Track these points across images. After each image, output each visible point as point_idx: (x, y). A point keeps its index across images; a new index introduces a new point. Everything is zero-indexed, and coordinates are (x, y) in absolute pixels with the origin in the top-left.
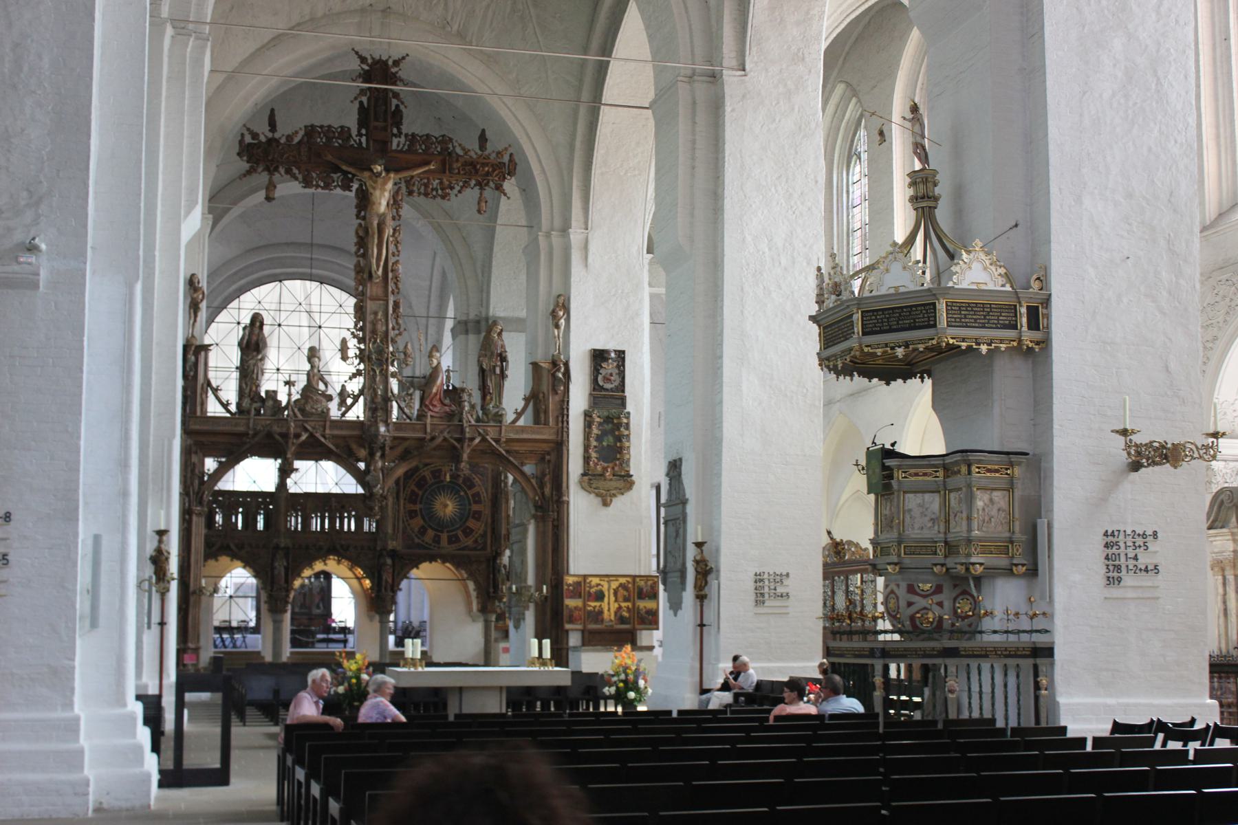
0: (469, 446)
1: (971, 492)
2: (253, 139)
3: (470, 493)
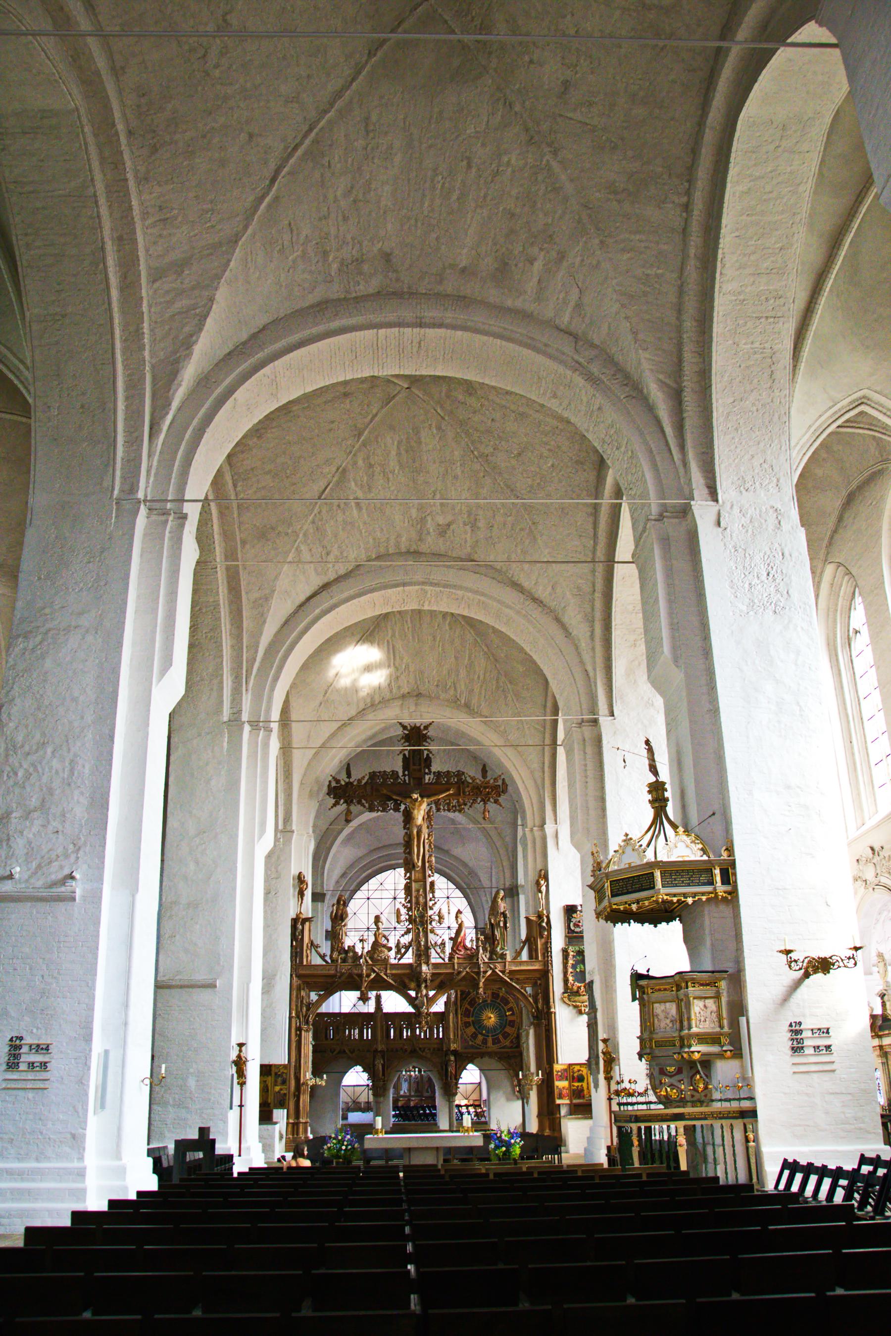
1: (689, 1001)
3: (506, 1008)
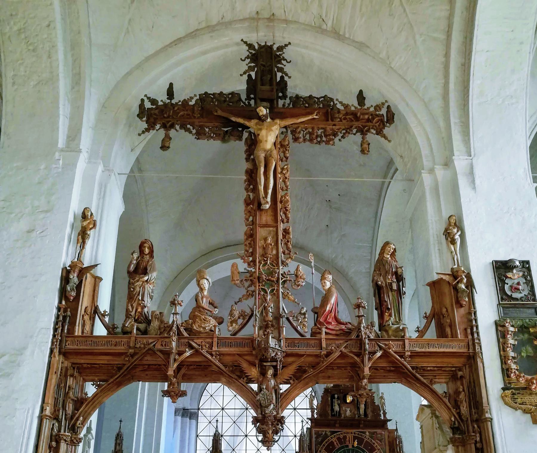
0: (370, 359)
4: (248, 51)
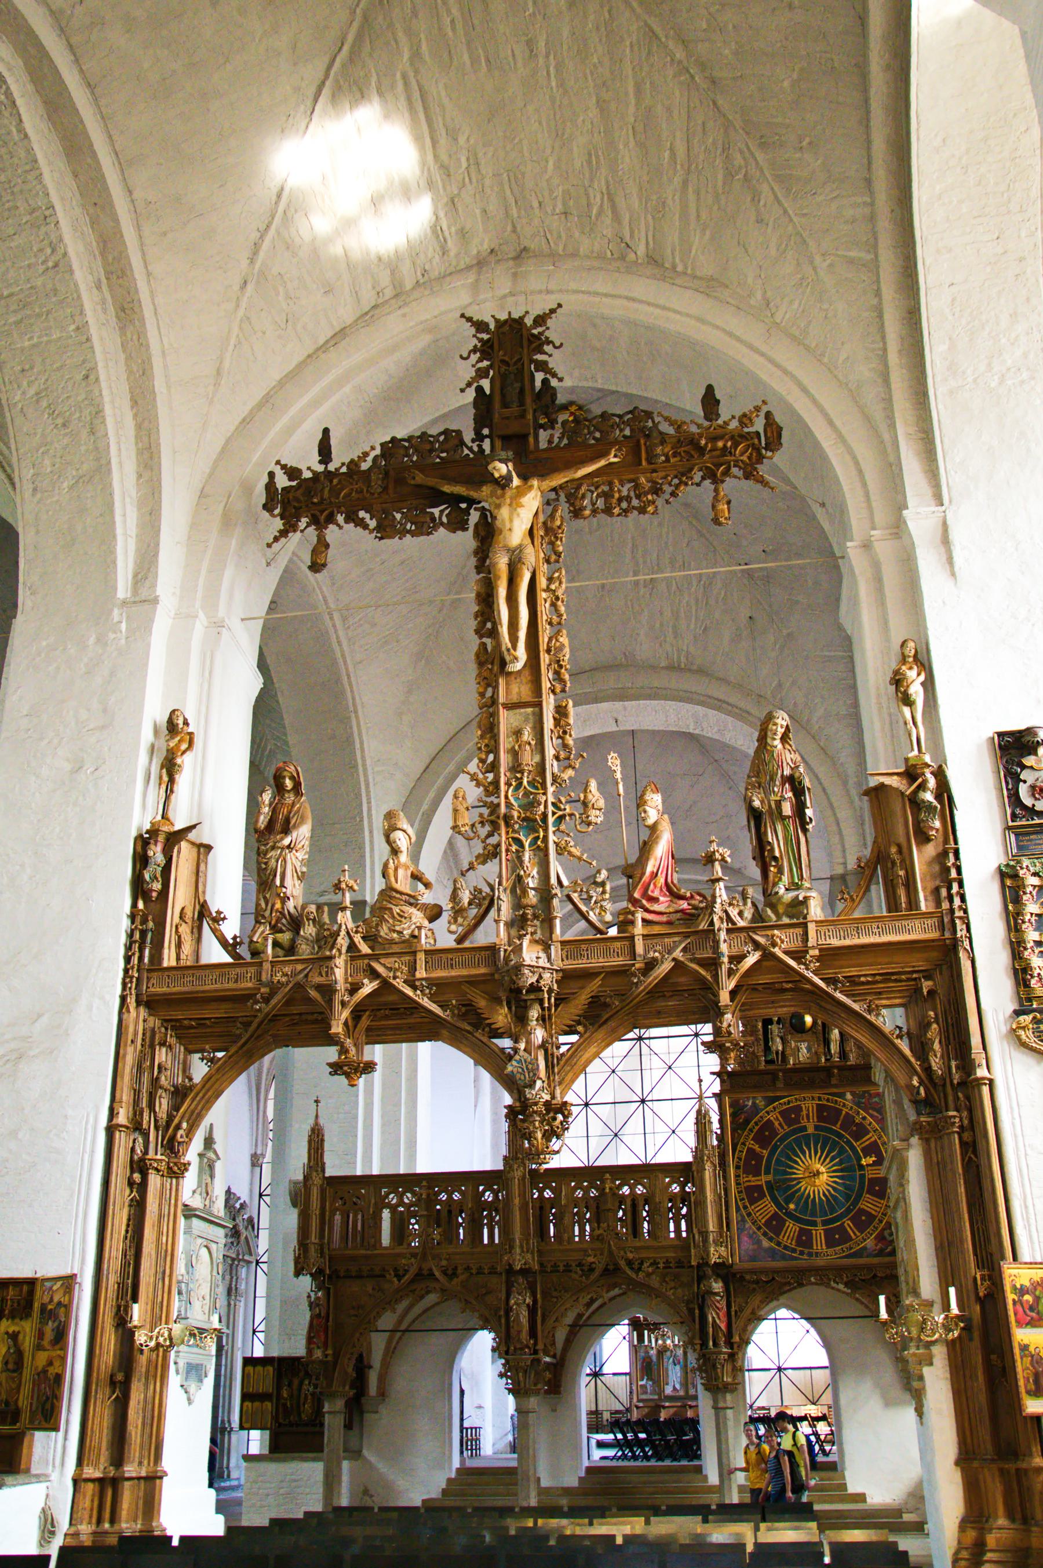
0: (731, 973)
2: (290, 480)
4: (474, 336)
